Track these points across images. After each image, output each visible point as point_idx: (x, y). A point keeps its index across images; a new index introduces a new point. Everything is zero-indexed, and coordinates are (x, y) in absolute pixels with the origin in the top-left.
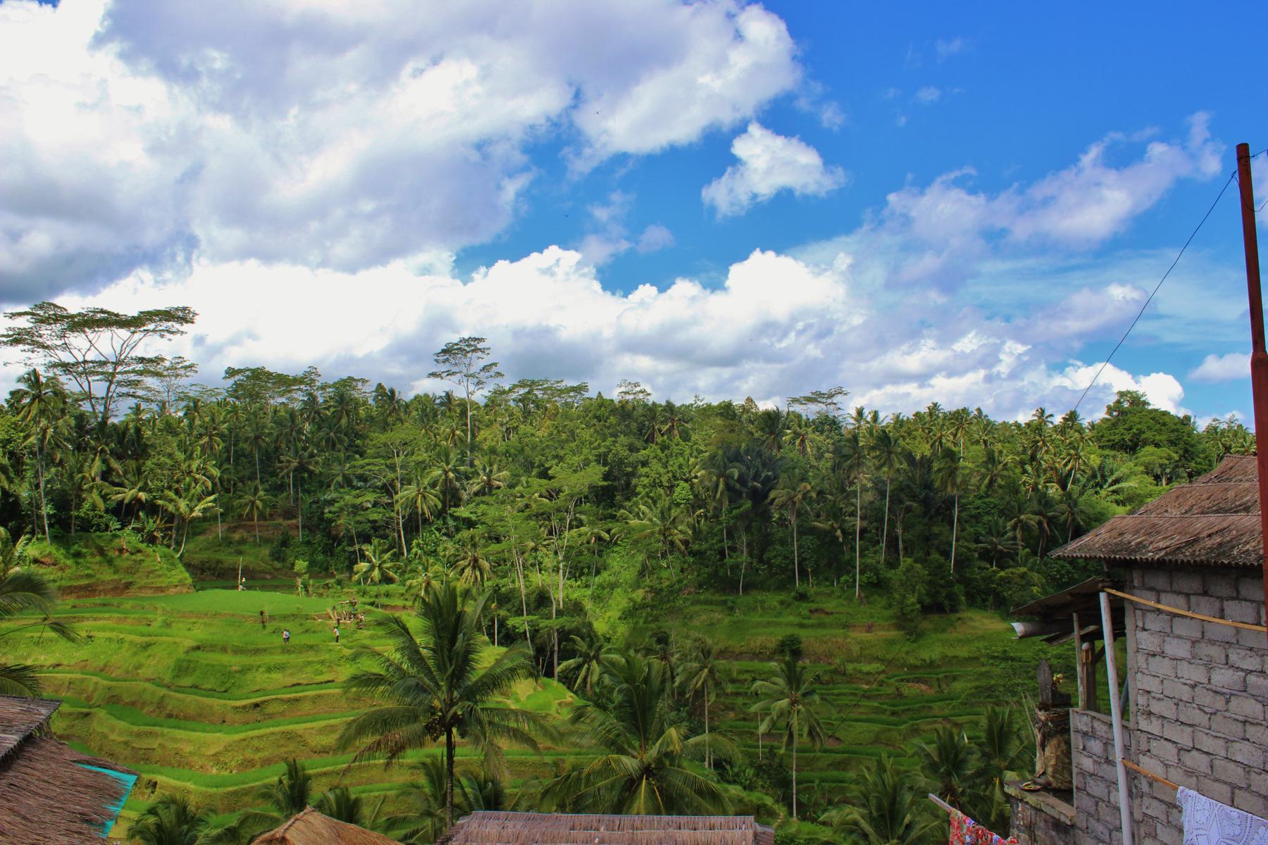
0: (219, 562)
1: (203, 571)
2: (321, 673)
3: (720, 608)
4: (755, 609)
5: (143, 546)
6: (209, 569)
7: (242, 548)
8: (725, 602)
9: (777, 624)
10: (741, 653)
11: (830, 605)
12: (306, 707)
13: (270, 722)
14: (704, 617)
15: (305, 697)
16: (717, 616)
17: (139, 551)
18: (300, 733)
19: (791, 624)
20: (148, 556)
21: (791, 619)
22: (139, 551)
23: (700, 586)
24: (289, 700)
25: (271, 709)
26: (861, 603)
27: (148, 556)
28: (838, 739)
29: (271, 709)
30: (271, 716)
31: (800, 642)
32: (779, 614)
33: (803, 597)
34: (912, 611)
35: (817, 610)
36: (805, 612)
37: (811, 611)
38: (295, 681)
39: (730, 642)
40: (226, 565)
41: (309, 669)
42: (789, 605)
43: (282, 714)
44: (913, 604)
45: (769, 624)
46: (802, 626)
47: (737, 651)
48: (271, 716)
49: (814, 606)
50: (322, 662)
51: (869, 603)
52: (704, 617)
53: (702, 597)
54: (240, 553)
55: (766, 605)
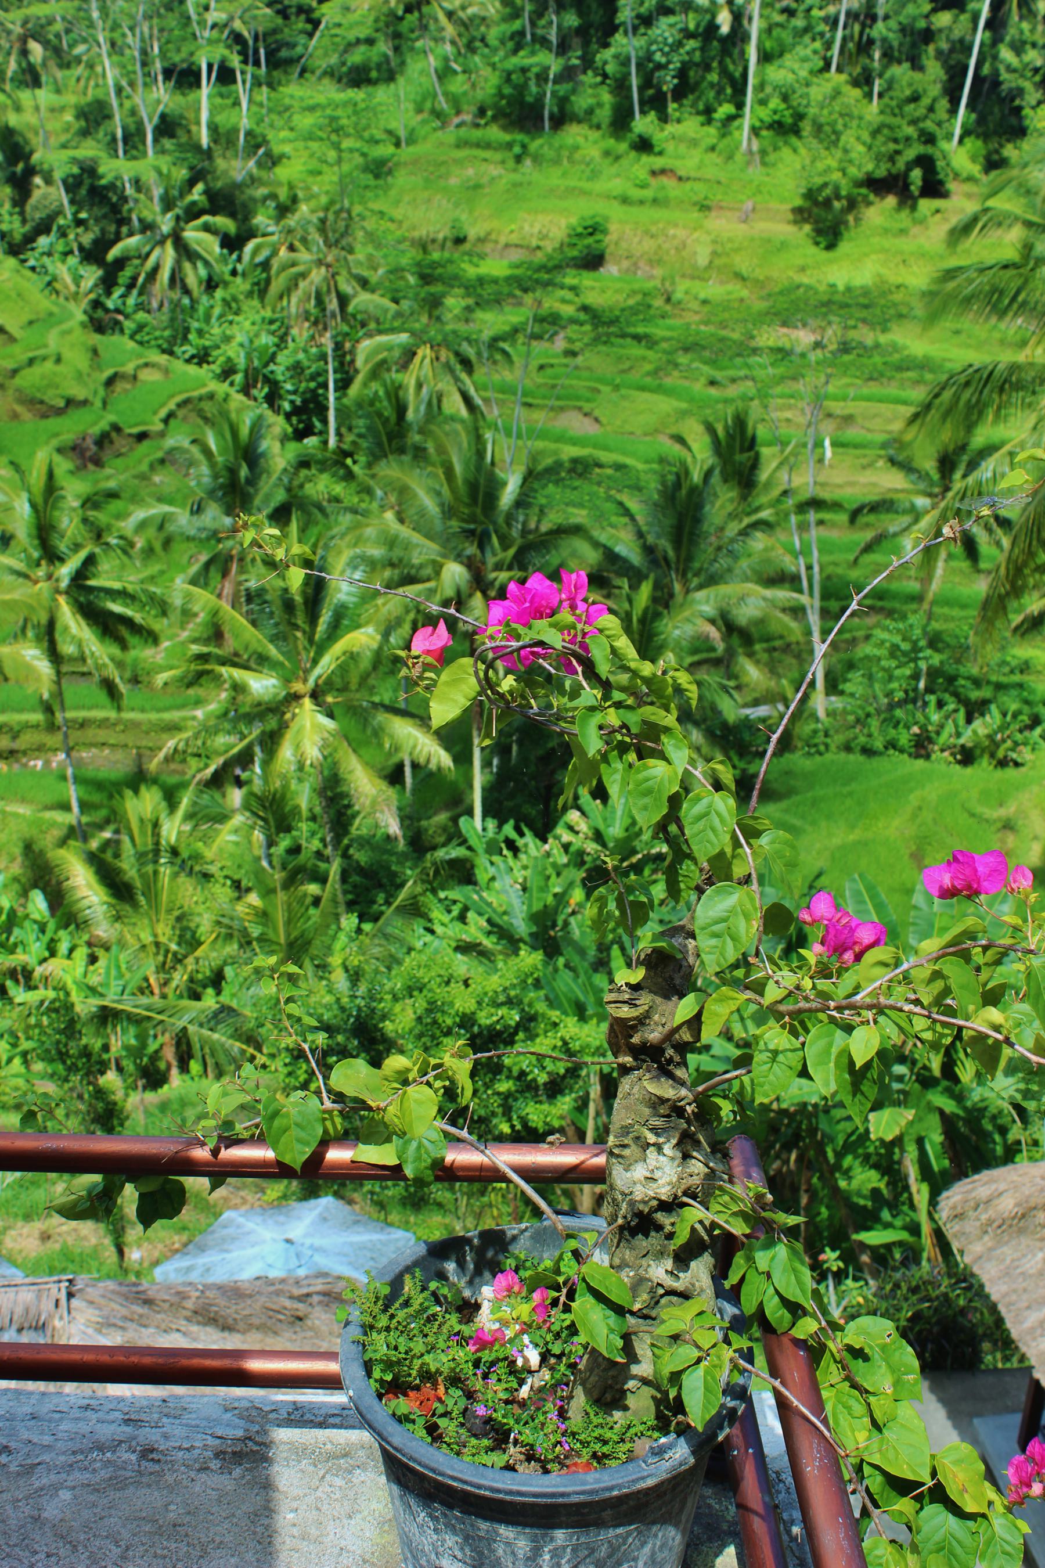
3: (498, 156)
4: (556, 162)
8: (509, 146)
9: (583, 193)
10: (507, 246)
11: (688, 162)
14: (470, 172)
16: (495, 171)
19: (608, 197)
21: (617, 185)
23: (482, 111)
26: (748, 163)
28: (597, 420)
31: (605, 232)
32: (595, 175)
33: (644, 145)
34: (825, 185)
35: (663, 172)
36: (643, 174)
37: (653, 173)
39: (495, 224)
42: (617, 158)
44: (828, 170)
45: (570, 191)
46: (625, 200)
47: (503, 240)
49: (658, 162)
51: (764, 164)
52: (470, 172)
53: (477, 134)
55: (577, 156)
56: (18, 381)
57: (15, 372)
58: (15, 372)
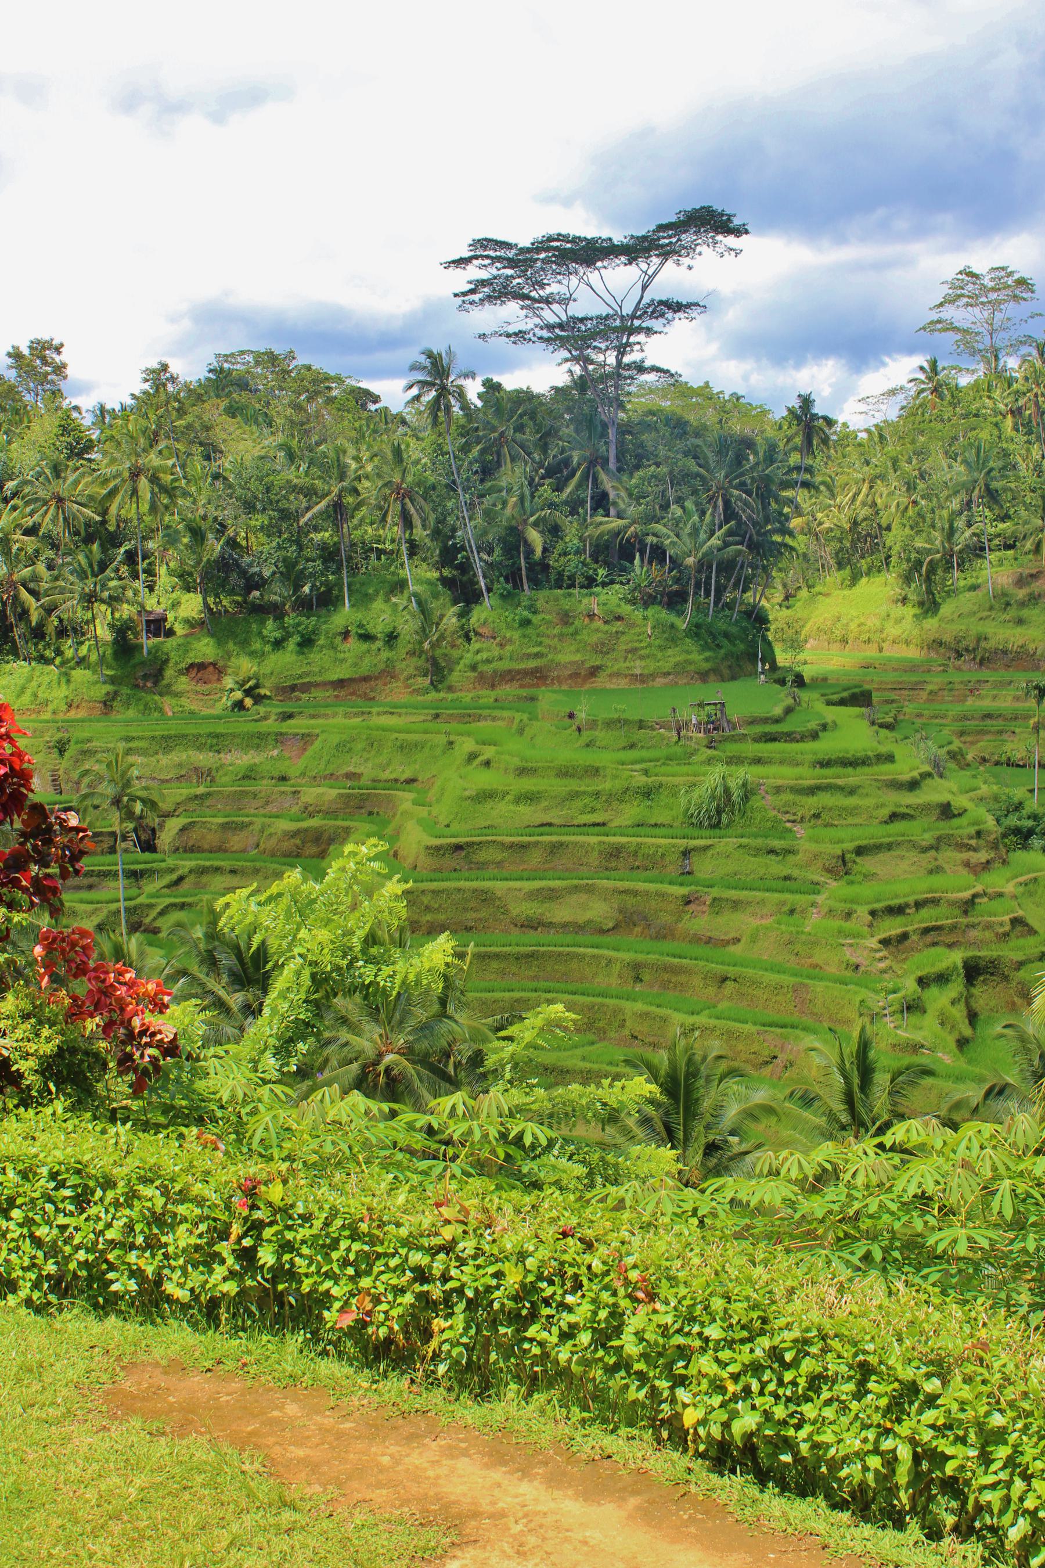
0: (981, 638)
1: (959, 655)
2: (593, 810)
5: (626, 609)
6: (967, 650)
7: (1025, 613)
12: (535, 857)
13: (473, 874)
15: (537, 843)
17: (619, 618)
18: (499, 894)
20: (633, 625)
22: (619, 618)
24: (512, 846)
25: (483, 856)
27: (633, 625)
29: (483, 856)
30: (482, 866)
38: (547, 819)
40: (991, 644)
41: (579, 803)
43: (499, 864)
48: (482, 866)
50: (597, 795)
54: (1020, 622)
56: (1022, 974)
57: (1020, 965)
58: (1020, 965)
